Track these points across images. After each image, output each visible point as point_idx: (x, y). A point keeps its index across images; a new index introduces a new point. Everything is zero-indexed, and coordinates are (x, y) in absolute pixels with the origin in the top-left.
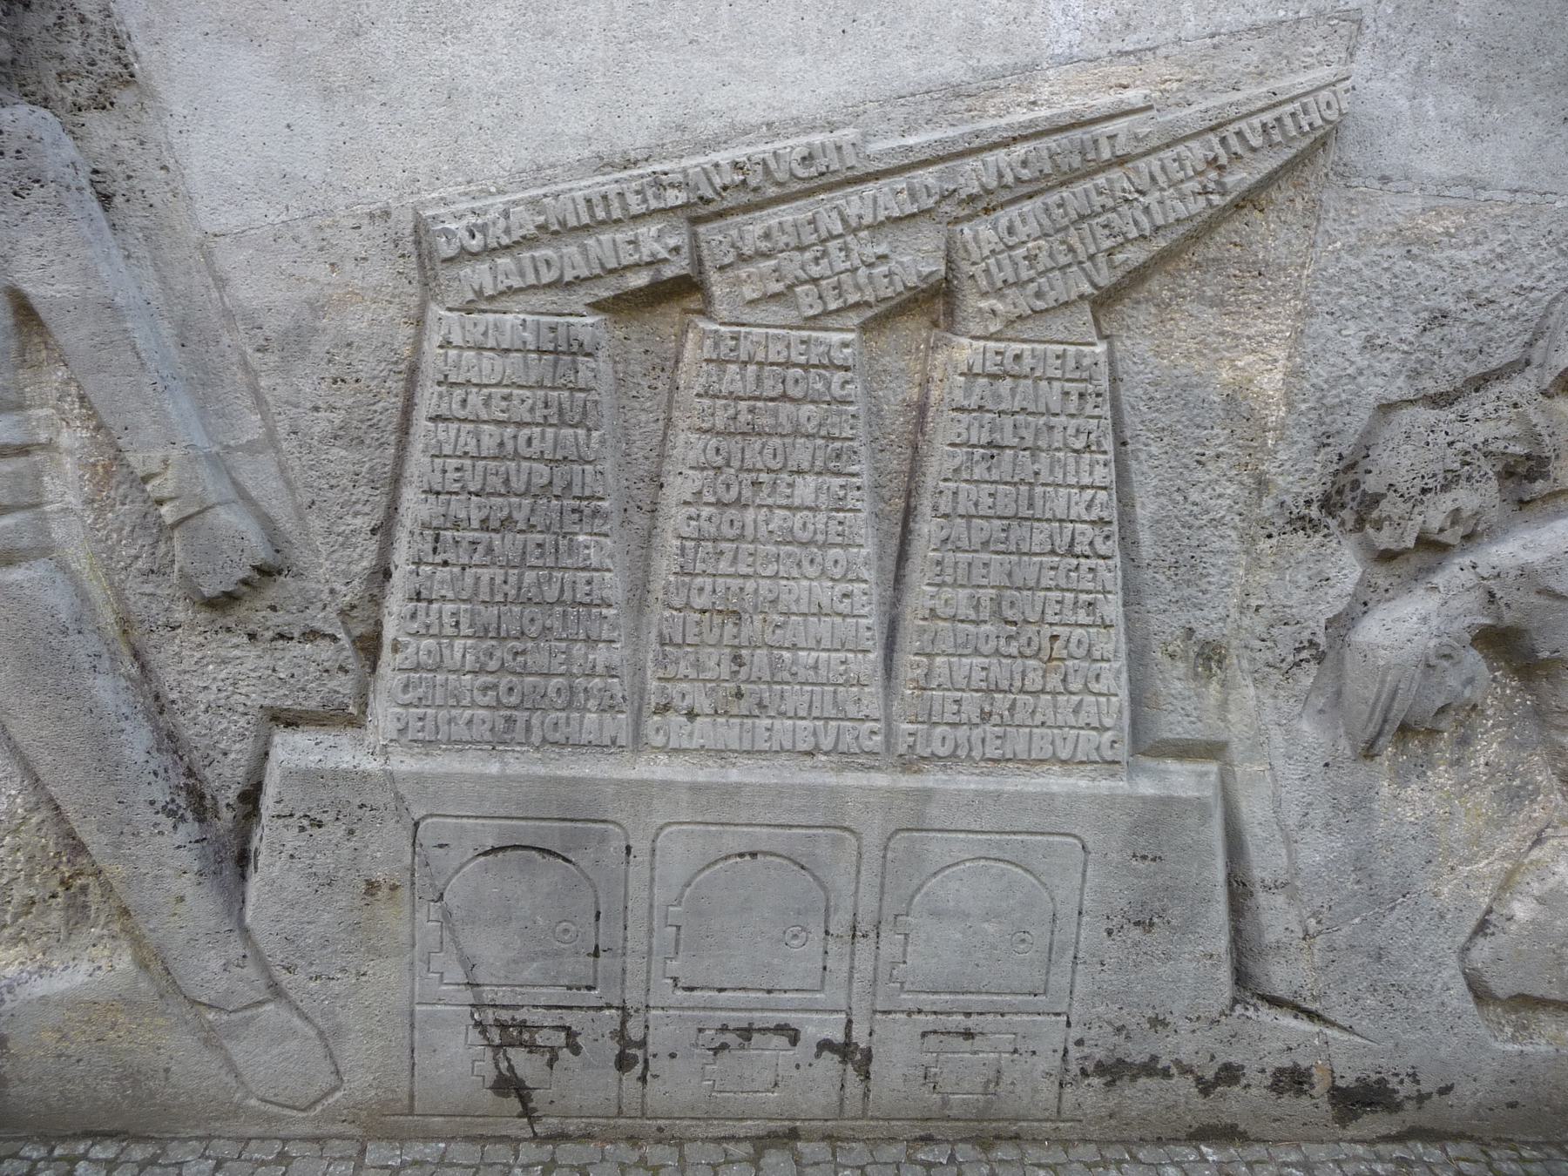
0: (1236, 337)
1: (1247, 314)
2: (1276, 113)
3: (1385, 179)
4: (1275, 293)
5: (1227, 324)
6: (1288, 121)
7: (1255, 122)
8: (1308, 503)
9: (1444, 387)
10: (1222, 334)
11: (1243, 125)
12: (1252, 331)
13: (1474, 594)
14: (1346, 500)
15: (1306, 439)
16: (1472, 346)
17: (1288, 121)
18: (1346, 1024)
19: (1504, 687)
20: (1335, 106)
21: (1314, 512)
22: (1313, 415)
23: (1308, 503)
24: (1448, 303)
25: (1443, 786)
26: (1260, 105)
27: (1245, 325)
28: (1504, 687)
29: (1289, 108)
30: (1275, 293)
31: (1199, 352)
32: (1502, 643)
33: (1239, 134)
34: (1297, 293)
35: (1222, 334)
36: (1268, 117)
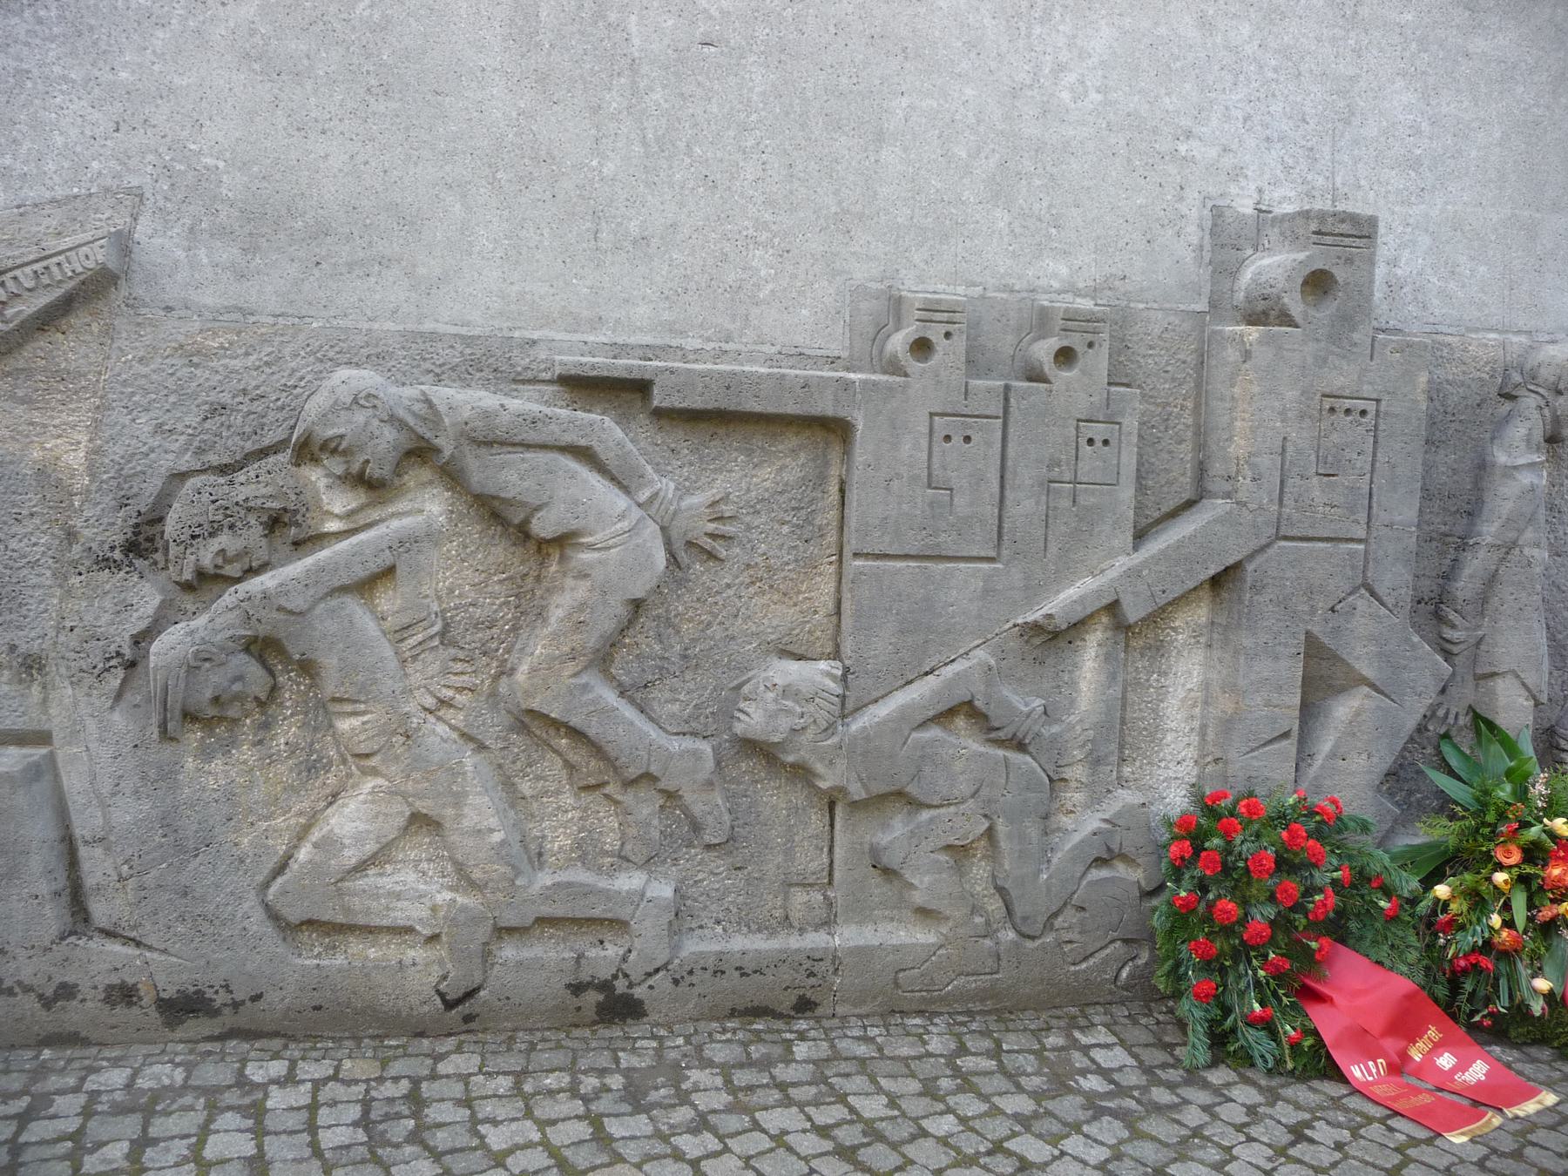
0: (45, 426)
1: (53, 409)
2: (45, 263)
3: (169, 309)
4: (76, 393)
5: (37, 417)
6: (55, 269)
7: (28, 270)
8: (112, 548)
9: (226, 460)
10: (32, 424)
11: (17, 273)
12: (57, 422)
13: (236, 612)
14: (141, 543)
15: (108, 501)
16: (248, 429)
17: (55, 269)
18: (162, 947)
19: (298, 684)
20: (92, 258)
21: (117, 555)
22: (114, 483)
23: (112, 548)
24: (226, 398)
25: (245, 762)
26: (32, 257)
27: (52, 418)
28: (298, 684)
29: (55, 260)
30: (76, 393)
31: (12, 438)
32: (263, 648)
33: (15, 278)
34: (95, 393)
35: (32, 424)
36: (36, 267)
